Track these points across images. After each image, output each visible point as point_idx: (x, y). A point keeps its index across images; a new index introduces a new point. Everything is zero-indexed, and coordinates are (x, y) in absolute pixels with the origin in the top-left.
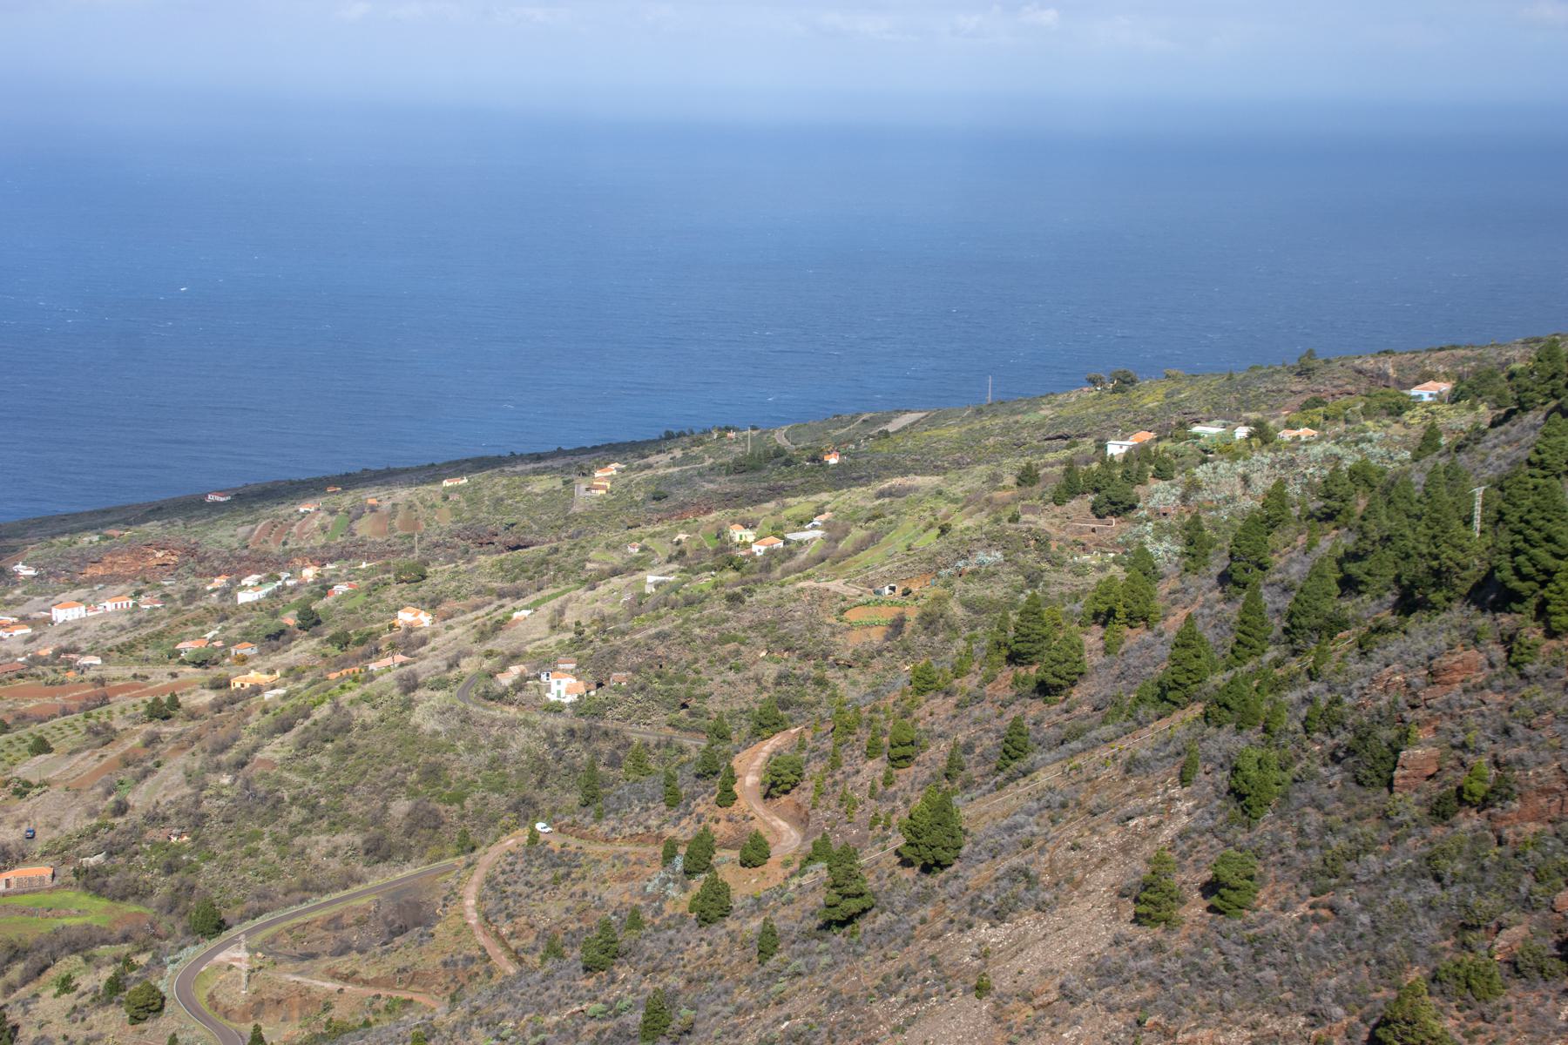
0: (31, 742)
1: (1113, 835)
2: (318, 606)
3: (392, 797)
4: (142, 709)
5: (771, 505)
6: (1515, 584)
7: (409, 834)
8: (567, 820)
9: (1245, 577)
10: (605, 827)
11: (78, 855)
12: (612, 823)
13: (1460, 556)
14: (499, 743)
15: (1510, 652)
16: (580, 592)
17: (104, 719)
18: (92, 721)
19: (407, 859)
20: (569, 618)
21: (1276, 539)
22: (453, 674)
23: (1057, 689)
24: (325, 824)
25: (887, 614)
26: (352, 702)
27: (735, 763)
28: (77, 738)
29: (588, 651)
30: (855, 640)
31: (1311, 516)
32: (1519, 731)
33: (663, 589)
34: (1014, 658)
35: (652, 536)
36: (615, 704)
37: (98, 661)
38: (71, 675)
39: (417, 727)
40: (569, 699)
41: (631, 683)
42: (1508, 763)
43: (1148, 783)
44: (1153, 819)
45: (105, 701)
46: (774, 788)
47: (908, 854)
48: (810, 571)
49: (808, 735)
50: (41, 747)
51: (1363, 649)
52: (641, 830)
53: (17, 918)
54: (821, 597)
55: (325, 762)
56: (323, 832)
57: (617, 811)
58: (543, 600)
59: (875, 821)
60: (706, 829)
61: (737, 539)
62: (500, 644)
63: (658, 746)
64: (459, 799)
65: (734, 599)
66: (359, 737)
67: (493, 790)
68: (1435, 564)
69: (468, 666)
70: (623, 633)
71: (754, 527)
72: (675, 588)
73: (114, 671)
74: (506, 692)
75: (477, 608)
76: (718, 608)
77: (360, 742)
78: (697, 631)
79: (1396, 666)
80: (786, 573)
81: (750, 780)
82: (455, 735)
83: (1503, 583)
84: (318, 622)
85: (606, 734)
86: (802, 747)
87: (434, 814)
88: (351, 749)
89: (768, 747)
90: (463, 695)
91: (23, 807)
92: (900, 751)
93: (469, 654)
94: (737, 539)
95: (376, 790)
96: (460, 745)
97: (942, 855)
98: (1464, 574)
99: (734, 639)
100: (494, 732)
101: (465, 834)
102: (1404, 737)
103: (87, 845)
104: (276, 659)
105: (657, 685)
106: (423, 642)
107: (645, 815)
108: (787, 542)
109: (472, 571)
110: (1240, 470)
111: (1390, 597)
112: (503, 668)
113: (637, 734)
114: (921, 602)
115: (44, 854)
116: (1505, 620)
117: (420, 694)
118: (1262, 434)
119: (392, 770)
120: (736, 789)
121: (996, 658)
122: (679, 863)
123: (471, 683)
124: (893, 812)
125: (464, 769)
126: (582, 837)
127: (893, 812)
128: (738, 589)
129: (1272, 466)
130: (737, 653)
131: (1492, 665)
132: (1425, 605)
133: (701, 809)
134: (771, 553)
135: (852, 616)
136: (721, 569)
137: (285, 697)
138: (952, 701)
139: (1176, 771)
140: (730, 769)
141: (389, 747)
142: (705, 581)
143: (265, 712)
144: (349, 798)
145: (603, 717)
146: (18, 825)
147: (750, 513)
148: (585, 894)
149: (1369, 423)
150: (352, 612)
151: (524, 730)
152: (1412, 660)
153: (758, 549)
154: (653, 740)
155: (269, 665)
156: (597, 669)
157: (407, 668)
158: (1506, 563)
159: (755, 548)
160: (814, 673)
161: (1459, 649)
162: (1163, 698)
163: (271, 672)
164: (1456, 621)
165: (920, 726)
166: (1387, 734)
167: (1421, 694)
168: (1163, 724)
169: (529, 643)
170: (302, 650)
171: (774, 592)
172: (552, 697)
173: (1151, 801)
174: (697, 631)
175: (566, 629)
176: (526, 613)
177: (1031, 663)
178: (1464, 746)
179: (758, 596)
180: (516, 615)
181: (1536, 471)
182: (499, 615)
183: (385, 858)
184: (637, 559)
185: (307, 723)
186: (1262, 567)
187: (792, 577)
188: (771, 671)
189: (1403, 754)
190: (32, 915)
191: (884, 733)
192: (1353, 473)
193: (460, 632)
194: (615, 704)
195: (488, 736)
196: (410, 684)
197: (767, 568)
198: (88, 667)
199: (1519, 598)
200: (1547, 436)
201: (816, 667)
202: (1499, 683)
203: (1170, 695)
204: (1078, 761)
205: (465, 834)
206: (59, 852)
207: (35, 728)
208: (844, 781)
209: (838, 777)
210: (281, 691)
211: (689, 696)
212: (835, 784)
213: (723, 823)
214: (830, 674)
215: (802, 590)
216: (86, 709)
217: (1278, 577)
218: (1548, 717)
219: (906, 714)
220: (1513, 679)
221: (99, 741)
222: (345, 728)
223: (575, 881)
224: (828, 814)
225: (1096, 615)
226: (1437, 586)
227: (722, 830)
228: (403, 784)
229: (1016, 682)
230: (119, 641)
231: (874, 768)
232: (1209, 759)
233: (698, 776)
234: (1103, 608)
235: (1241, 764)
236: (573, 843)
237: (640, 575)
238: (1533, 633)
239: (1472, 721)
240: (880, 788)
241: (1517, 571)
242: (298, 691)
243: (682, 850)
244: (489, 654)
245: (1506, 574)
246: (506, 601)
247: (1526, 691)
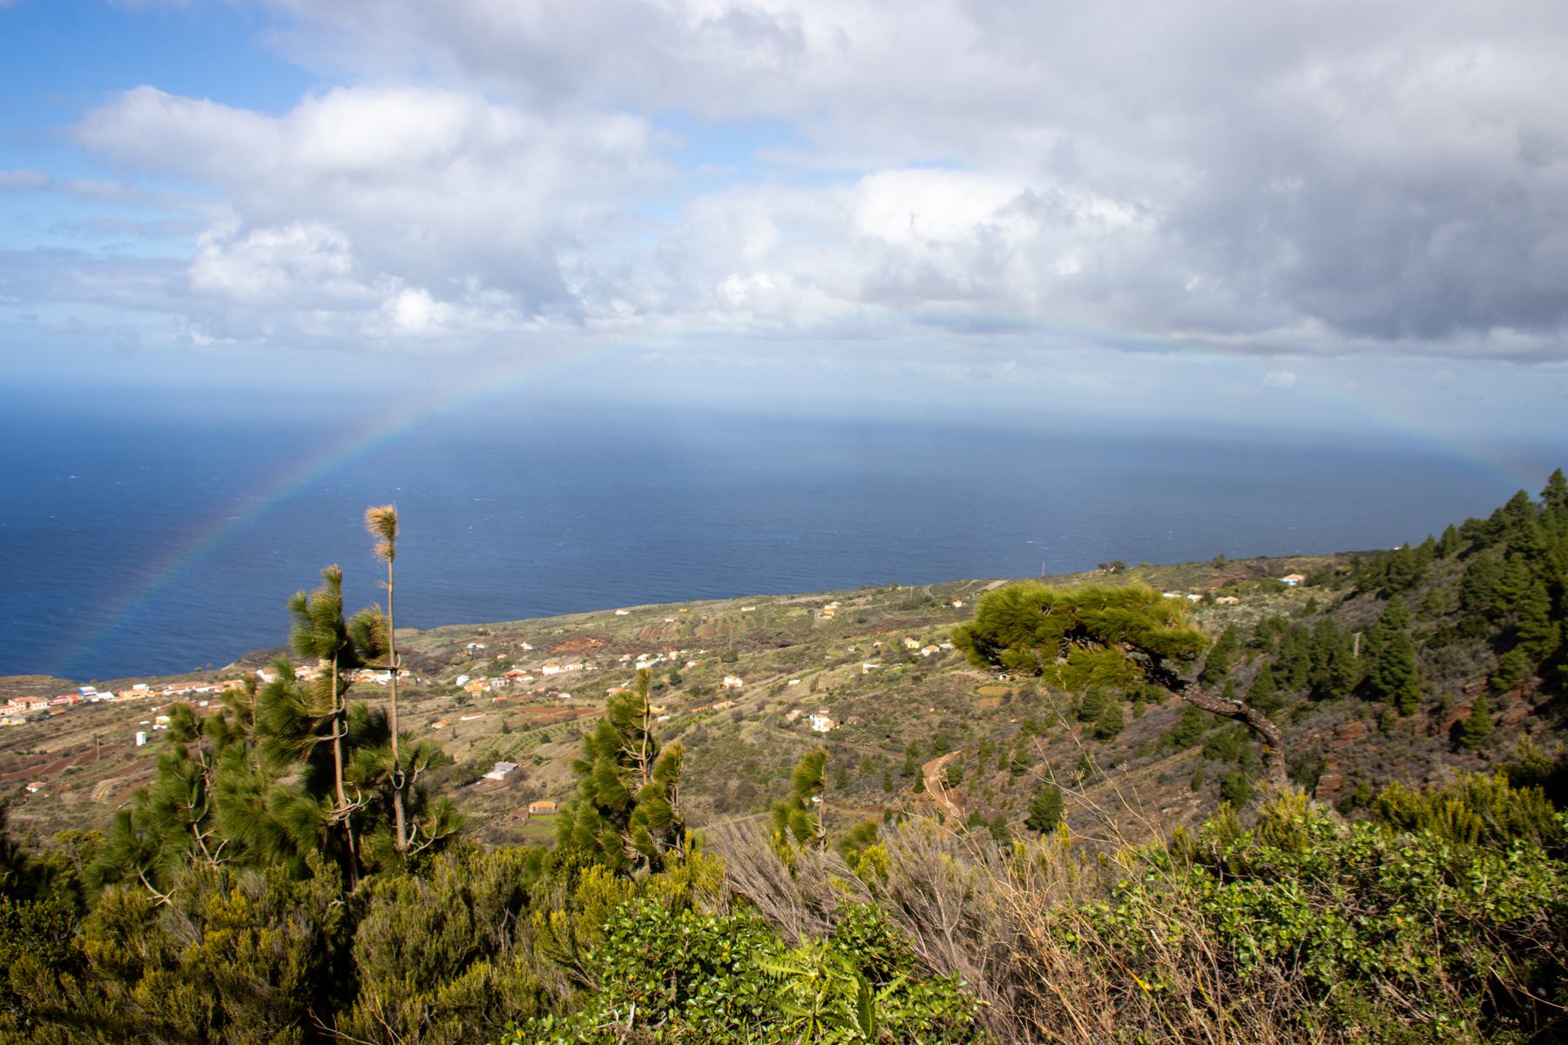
0: (541, 736)
1: (1154, 818)
2: (680, 672)
3: (729, 778)
4: (594, 723)
5: (927, 628)
6: (1383, 686)
7: (738, 798)
8: (829, 796)
9: (1213, 677)
10: (850, 801)
12: (855, 799)
13: (1349, 670)
14: (787, 752)
15: (1380, 724)
16: (826, 671)
17: (575, 727)
18: (569, 728)
19: (737, 812)
20: (821, 685)
21: (1229, 657)
22: (761, 713)
23: (1107, 736)
24: (693, 790)
25: (1002, 691)
26: (706, 725)
27: (923, 769)
28: (563, 736)
29: (836, 704)
31: (1248, 645)
32: (1387, 767)
33: (873, 672)
34: (1082, 718)
35: (862, 642)
36: (850, 733)
37: (568, 696)
38: (557, 702)
39: (742, 741)
40: (825, 730)
42: (1381, 784)
43: (1173, 789)
44: (1177, 809)
45: (575, 717)
47: (1033, 822)
48: (957, 665)
49: (965, 755)
50: (546, 739)
51: (1295, 719)
52: (871, 803)
53: (538, 827)
54: (965, 680)
55: (694, 757)
56: (693, 794)
58: (806, 675)
59: (1004, 805)
61: (909, 646)
62: (783, 697)
63: (874, 758)
64: (765, 781)
65: (916, 679)
67: (784, 777)
68: (1335, 674)
69: (769, 709)
70: (855, 695)
71: (918, 640)
72: (880, 671)
73: (578, 702)
74: (791, 724)
75: (768, 678)
76: (906, 683)
77: (712, 747)
78: (896, 696)
79: (1315, 729)
80: (944, 666)
82: (763, 746)
83: (1375, 686)
84: (680, 682)
85: (845, 750)
86: (961, 762)
87: (752, 788)
88: (707, 751)
89: (941, 761)
90: (767, 724)
91: (540, 770)
93: (769, 703)
94: (909, 646)
95: (721, 774)
96: (766, 752)
98: (1351, 680)
99: (916, 701)
100: (784, 745)
102: (1322, 768)
104: (660, 700)
105: (873, 724)
106: (740, 695)
108: (941, 649)
109: (763, 657)
110: (1197, 619)
111: (1306, 692)
112: (789, 711)
113: (862, 750)
114: (1021, 685)
115: (551, 795)
116: (1376, 706)
117: (744, 723)
118: (1208, 599)
119: (729, 763)
120: (925, 783)
121: (1072, 717)
123: (770, 719)
124: (1014, 799)
125: (767, 765)
126: (837, 805)
127: (1014, 799)
128: (918, 673)
129: (1215, 617)
130: (918, 709)
131: (1370, 730)
132: (1328, 696)
133: (905, 794)
134: (933, 654)
135: (982, 691)
136: (904, 662)
137: (670, 721)
138: (1047, 740)
139: (1189, 783)
141: (728, 751)
142: (897, 668)
143: (660, 728)
144: (706, 777)
145: (844, 740)
146: (538, 778)
147: (915, 632)
149: (1266, 596)
150: (698, 677)
151: (800, 746)
152: (1325, 726)
153: (926, 652)
155: (658, 703)
156: (840, 714)
157: (736, 709)
158: (1377, 674)
160: (961, 722)
161: (1351, 721)
162: (1177, 742)
163: (660, 707)
164: (1348, 706)
165: (1029, 753)
166: (1312, 766)
167: (1331, 745)
168: (1178, 757)
169: (802, 697)
170: (673, 696)
171: (938, 676)
172: (816, 728)
173: (1175, 799)
174: (896, 696)
175: (820, 691)
176: (797, 682)
177: (1092, 721)
178: (1355, 774)
179: (930, 678)
180: (791, 683)
181: (1385, 625)
182: (781, 682)
183: (726, 811)
184: (853, 655)
185: (683, 735)
186: (1223, 672)
187: (948, 668)
188: (937, 720)
189: (1321, 777)
190: (545, 826)
192: (1271, 622)
193: (759, 691)
194: (850, 733)
195: (781, 748)
196: (739, 717)
197: (932, 663)
198: (565, 699)
199: (1384, 694)
200: (1390, 606)
201: (962, 718)
202: (1374, 740)
203: (1182, 741)
206: (559, 795)
207: (542, 729)
208: (986, 782)
209: (983, 779)
210: (667, 718)
211: (891, 731)
212: (981, 783)
213: (917, 802)
214: (969, 722)
215: (953, 676)
216: (566, 721)
217: (1232, 678)
218: (1402, 759)
219: (1021, 746)
220: (1382, 738)
221: (574, 738)
222: (704, 739)
223: (835, 829)
224: (977, 800)
225: (1128, 696)
226: (1336, 686)
228: (735, 771)
229: (1084, 730)
230: (579, 685)
231: (1003, 776)
232: (1208, 777)
233: (902, 775)
234: (1133, 692)
235: (1228, 780)
236: (833, 809)
237: (858, 664)
238: (1392, 713)
239: (1360, 760)
240: (1007, 787)
241: (1384, 679)
242: (676, 718)
244: (781, 703)
245: (1378, 681)
246: (784, 674)
247: (1390, 745)
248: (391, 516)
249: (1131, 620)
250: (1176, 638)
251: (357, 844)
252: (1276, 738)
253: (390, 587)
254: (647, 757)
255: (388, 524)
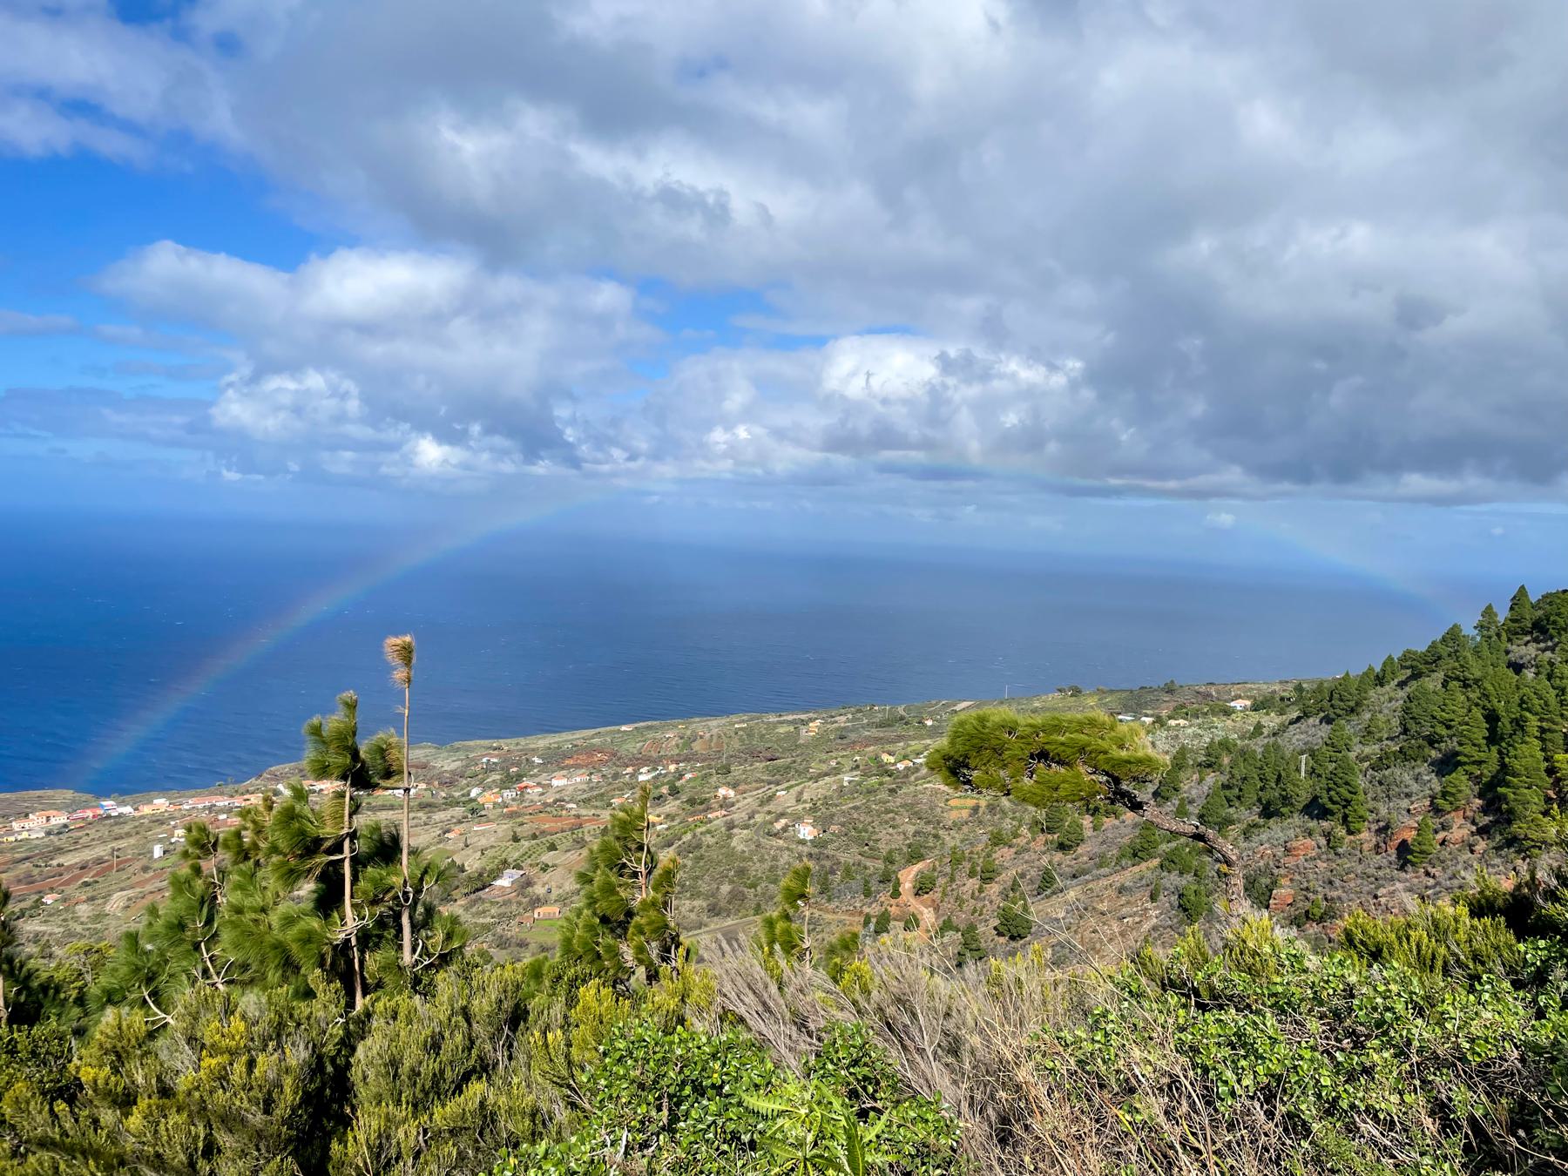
1: (1116, 927)
2: (678, 784)
3: (721, 883)
5: (902, 744)
6: (1330, 806)
7: (729, 902)
9: (1168, 794)
10: (832, 906)
11: (571, 902)
12: (837, 904)
14: (775, 858)
15: (1329, 841)
16: (810, 783)
17: (580, 835)
19: (728, 916)
20: (806, 796)
21: (1182, 775)
22: (752, 822)
23: (1070, 847)
24: (688, 895)
26: (701, 834)
27: (899, 876)
28: (568, 844)
29: (819, 814)
30: (954, 815)
31: (1200, 765)
32: (1337, 883)
33: (853, 784)
35: (842, 757)
37: (575, 806)
38: (564, 812)
39: (735, 848)
41: (840, 831)
42: (1332, 899)
43: (1132, 899)
44: (1137, 919)
45: (580, 826)
46: (921, 889)
47: (1001, 929)
49: (937, 863)
50: (553, 847)
51: (1246, 834)
52: (852, 908)
54: (936, 792)
55: (689, 863)
57: (838, 897)
58: (792, 787)
59: (975, 911)
60: (886, 910)
62: (771, 807)
63: (854, 865)
64: (754, 886)
65: (892, 791)
66: (706, 851)
68: (1284, 793)
69: (759, 818)
70: (837, 806)
72: (859, 784)
73: (583, 812)
75: (758, 789)
76: (883, 795)
79: (1267, 845)
80: (917, 779)
81: (907, 886)
83: (1323, 805)
84: (678, 792)
85: (828, 857)
87: (742, 893)
88: (702, 857)
90: (756, 833)
91: (546, 877)
92: (988, 875)
93: (759, 812)
97: (1022, 931)
98: (1298, 799)
99: (892, 811)
101: (759, 905)
102: (1275, 883)
103: (575, 898)
104: (659, 810)
106: (733, 805)
107: (853, 900)
109: (753, 770)
111: (1256, 809)
112: (777, 820)
113: (844, 858)
115: (556, 901)
116: (1325, 824)
117: (735, 831)
118: (1159, 721)
120: (901, 889)
121: (1036, 829)
122: (872, 927)
124: (984, 907)
127: (984, 907)
128: (894, 786)
129: (1167, 738)
130: (894, 819)
131: (1319, 847)
132: (1277, 813)
133: (883, 899)
134: (907, 768)
137: (667, 829)
138: (1013, 850)
139: (1148, 894)
140: (898, 879)
141: (720, 857)
142: (874, 780)
143: (658, 836)
144: (700, 882)
148: (823, 940)
149: (1215, 719)
150: (694, 788)
152: (1275, 843)
153: (901, 766)
154: (851, 861)
155: (657, 812)
156: (823, 822)
157: (729, 818)
158: (1325, 794)
159: (899, 765)
161: (1301, 838)
162: (1135, 855)
163: (659, 816)
164: (1298, 824)
165: (997, 862)
166: (1265, 881)
167: (1282, 861)
168: (1136, 869)
169: (789, 807)
170: (671, 806)
171: (912, 788)
172: (801, 837)
173: (1135, 909)
175: (805, 802)
176: (784, 793)
177: (1055, 833)
178: (1307, 889)
180: (778, 794)
181: (1330, 748)
182: (770, 793)
183: (717, 915)
184: (835, 768)
188: (911, 829)
189: (1274, 892)
191: (978, 865)
192: (1220, 743)
193: (750, 801)
195: (769, 855)
196: (731, 826)
197: (906, 776)
199: (1332, 814)
201: (934, 828)
202: (1324, 857)
203: (1139, 854)
204: (1090, 886)
205: (759, 905)
206: (563, 900)
207: (549, 838)
208: (958, 888)
209: (954, 886)
210: (665, 826)
211: (869, 840)
212: (953, 890)
213: (894, 907)
214: (941, 832)
216: (572, 830)
217: (1185, 795)
218: (1352, 876)
219: (989, 855)
220: (1332, 856)
222: (699, 846)
223: (818, 933)
224: (949, 906)
226: (1284, 805)
227: (893, 910)
228: (727, 877)
229: (1046, 842)
230: (585, 796)
231: (974, 883)
232: (1165, 889)
233: (880, 882)
235: (1185, 893)
236: (817, 914)
237: (839, 776)
238: (1341, 831)
239: (1311, 876)
240: (977, 894)
241: (1331, 799)
242: (674, 826)
243: (874, 920)
244: (769, 812)
245: (1325, 800)
246: (772, 786)
247: (1339, 861)
248: (410, 644)
249: (1089, 745)
250: (1132, 760)
251: (362, 962)
252: (1234, 858)
253: (407, 711)
254: (646, 869)
255: (406, 653)
